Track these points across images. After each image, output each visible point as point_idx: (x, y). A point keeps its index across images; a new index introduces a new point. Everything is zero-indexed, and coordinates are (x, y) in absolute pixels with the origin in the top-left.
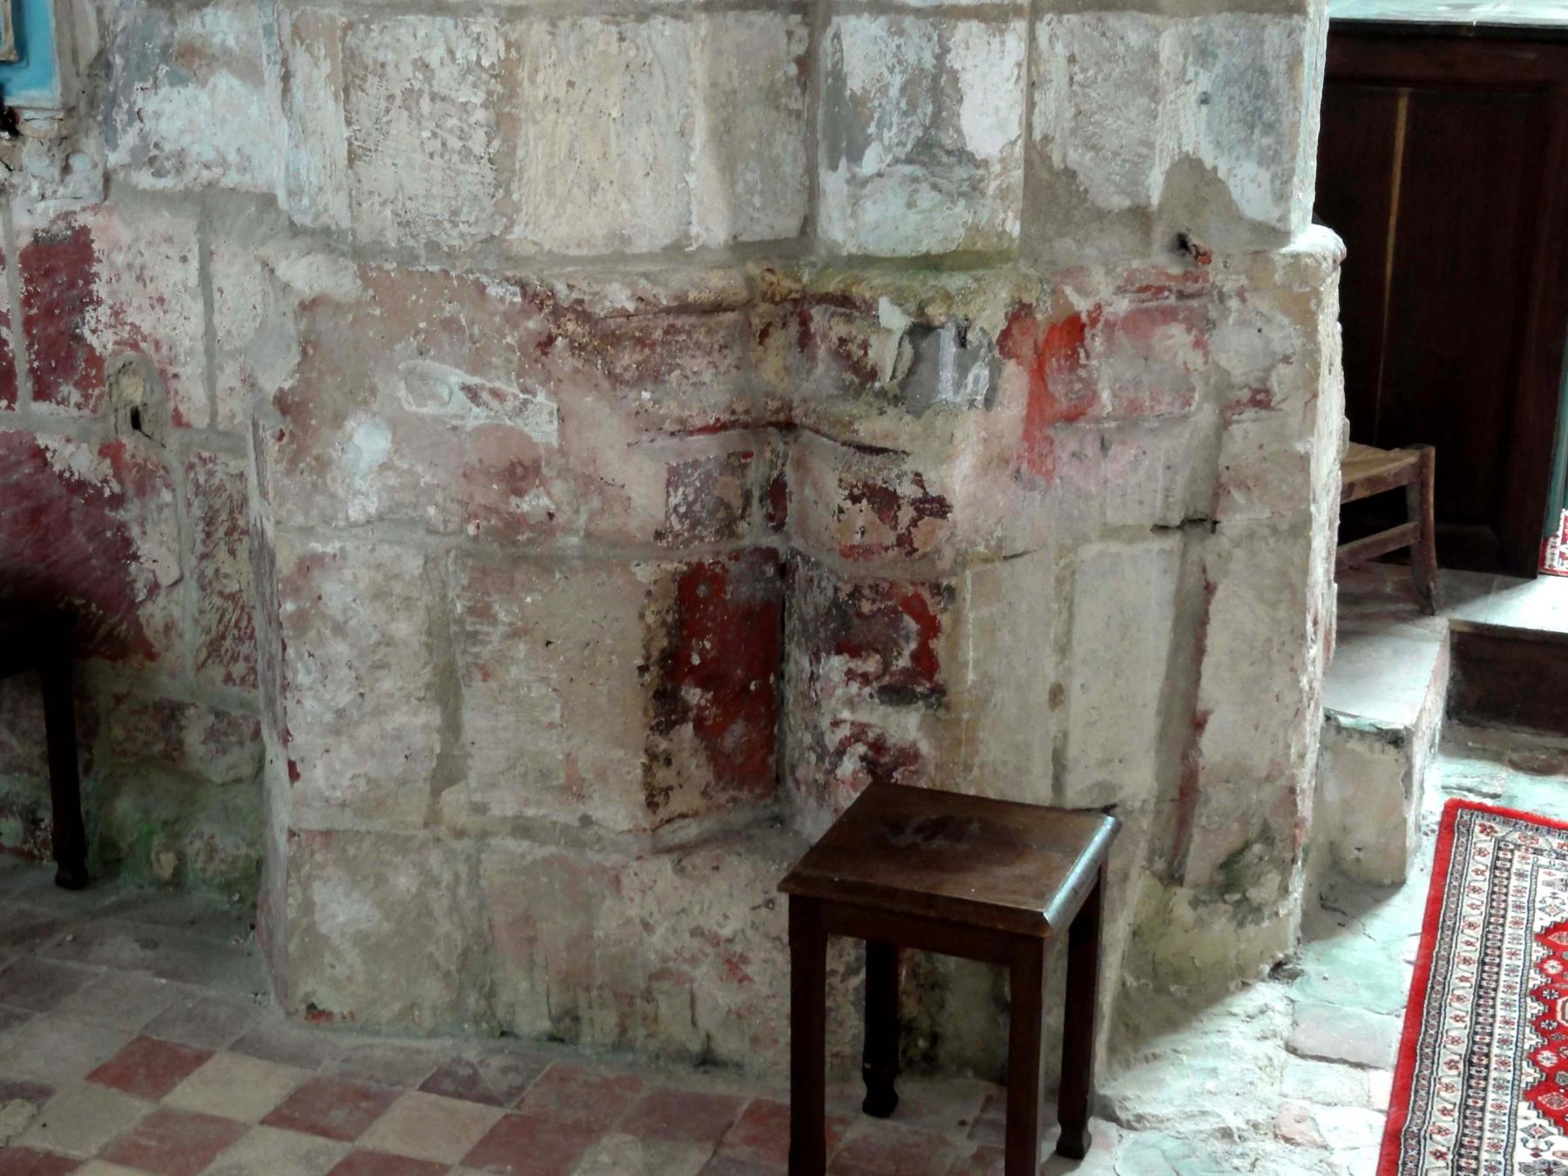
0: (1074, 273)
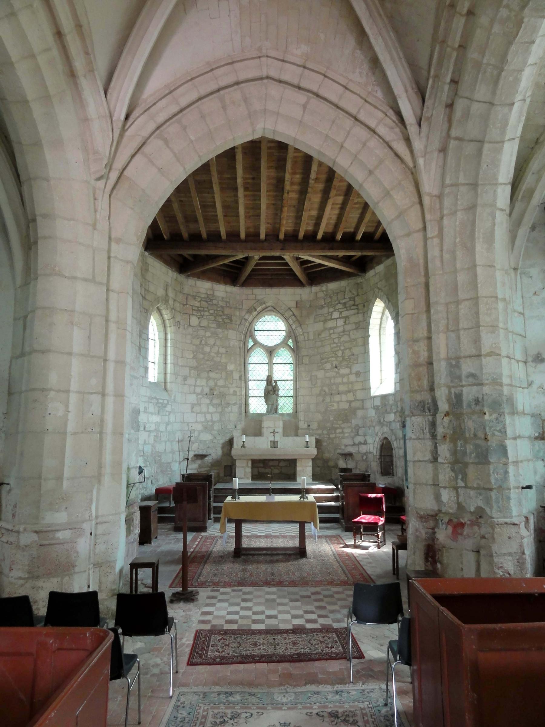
0: (463, 518)
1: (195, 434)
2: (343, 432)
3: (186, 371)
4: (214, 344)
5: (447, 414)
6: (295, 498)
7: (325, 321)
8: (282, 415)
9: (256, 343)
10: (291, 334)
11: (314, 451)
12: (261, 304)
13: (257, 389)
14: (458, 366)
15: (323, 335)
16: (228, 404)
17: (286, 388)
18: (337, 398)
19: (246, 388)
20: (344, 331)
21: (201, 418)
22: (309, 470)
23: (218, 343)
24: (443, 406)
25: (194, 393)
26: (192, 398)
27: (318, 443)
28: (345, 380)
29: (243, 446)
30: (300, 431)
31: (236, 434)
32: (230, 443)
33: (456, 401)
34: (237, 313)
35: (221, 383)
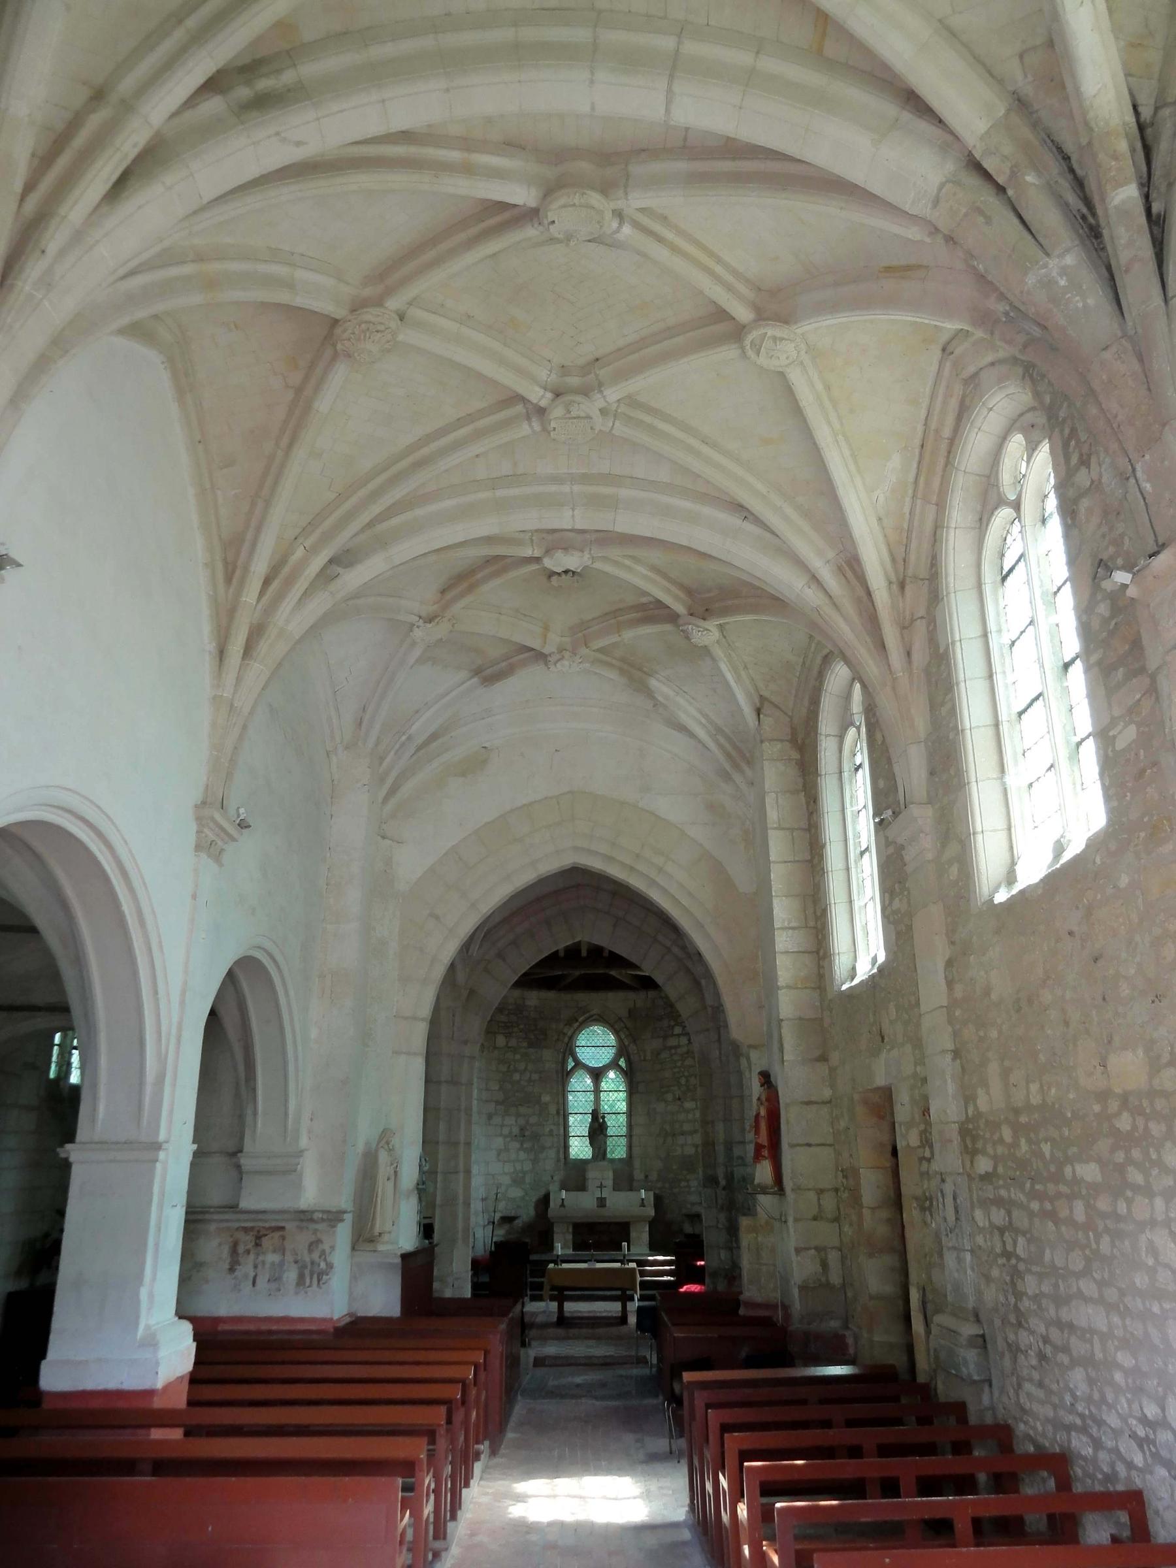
1: (502, 1190)
2: (688, 1186)
3: (491, 1107)
4: (526, 1069)
5: (724, 1189)
6: (617, 1265)
7: (665, 1037)
8: (613, 1161)
9: (578, 1064)
10: (622, 1051)
11: (652, 1213)
12: (584, 1013)
13: (579, 1125)
14: (731, 1149)
15: (664, 1055)
16: (543, 1148)
17: (616, 1125)
18: (681, 1140)
19: (566, 1126)
20: (688, 1052)
21: (508, 1168)
22: (645, 1237)
23: (530, 1067)
24: (723, 1182)
25: (501, 1135)
26: (499, 1142)
27: (658, 1200)
28: (690, 1116)
29: (563, 1205)
30: (635, 1184)
31: (553, 1188)
32: (545, 1201)
33: (730, 1177)
34: (554, 1026)
35: (533, 1120)
